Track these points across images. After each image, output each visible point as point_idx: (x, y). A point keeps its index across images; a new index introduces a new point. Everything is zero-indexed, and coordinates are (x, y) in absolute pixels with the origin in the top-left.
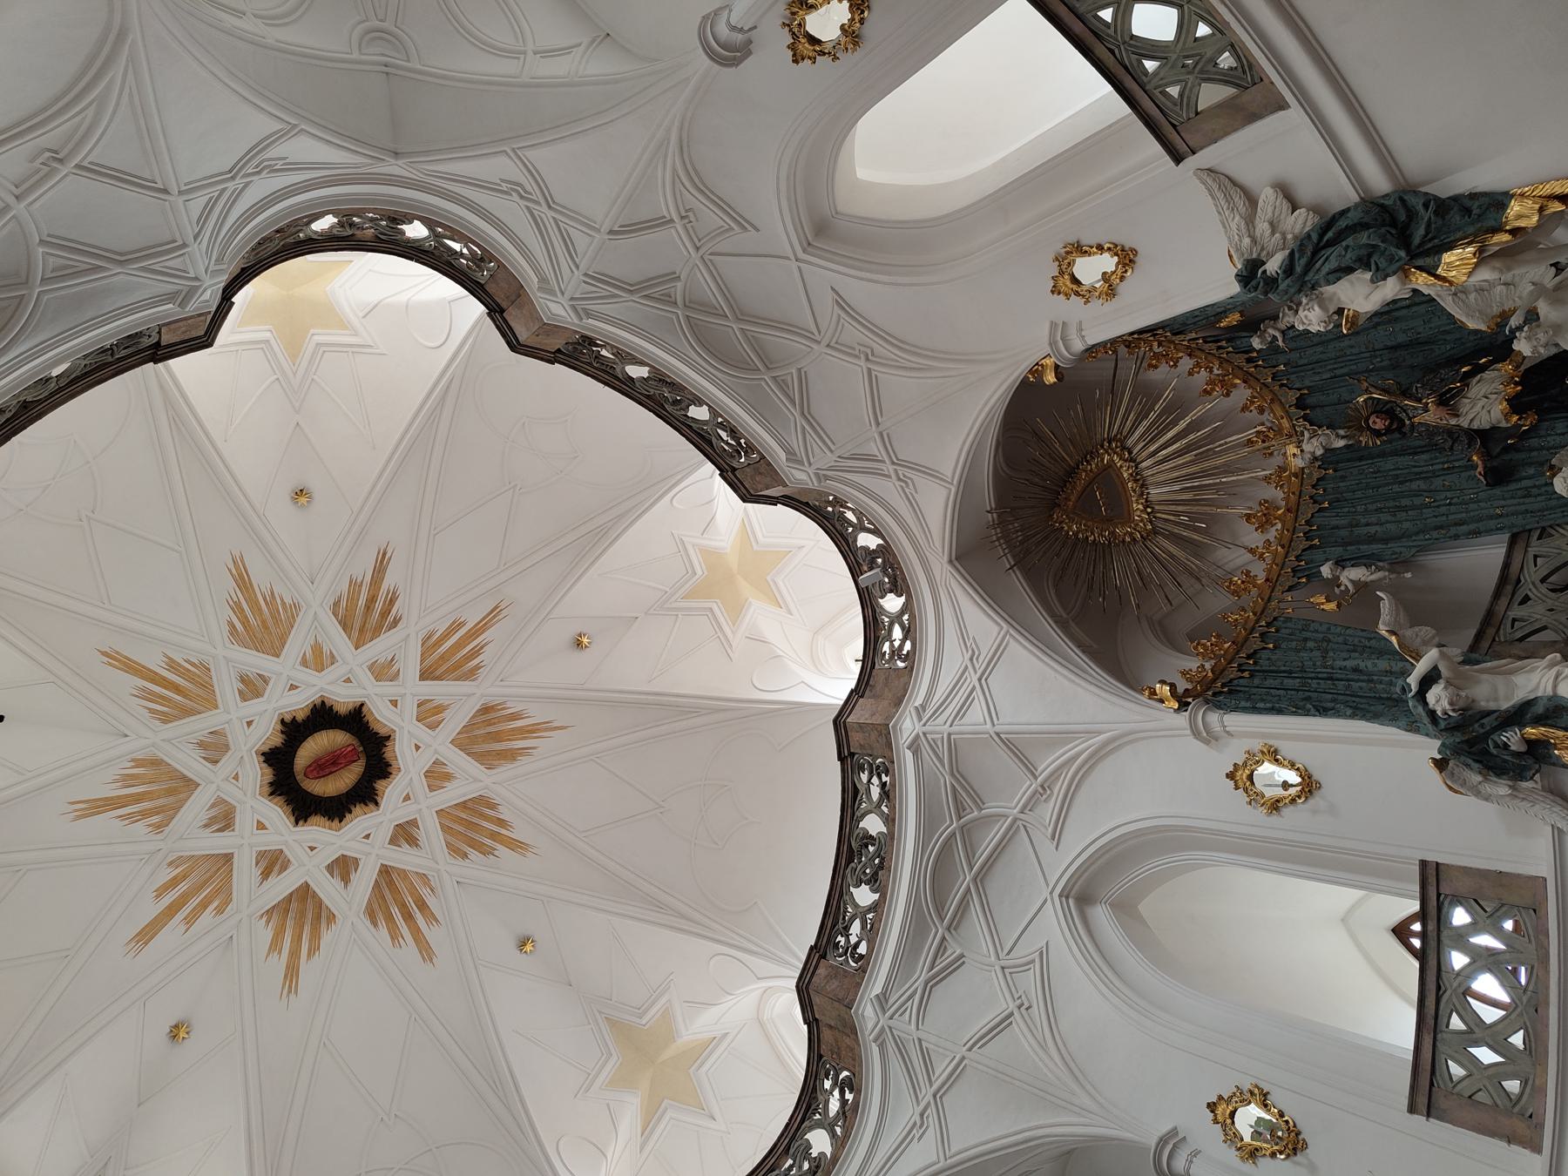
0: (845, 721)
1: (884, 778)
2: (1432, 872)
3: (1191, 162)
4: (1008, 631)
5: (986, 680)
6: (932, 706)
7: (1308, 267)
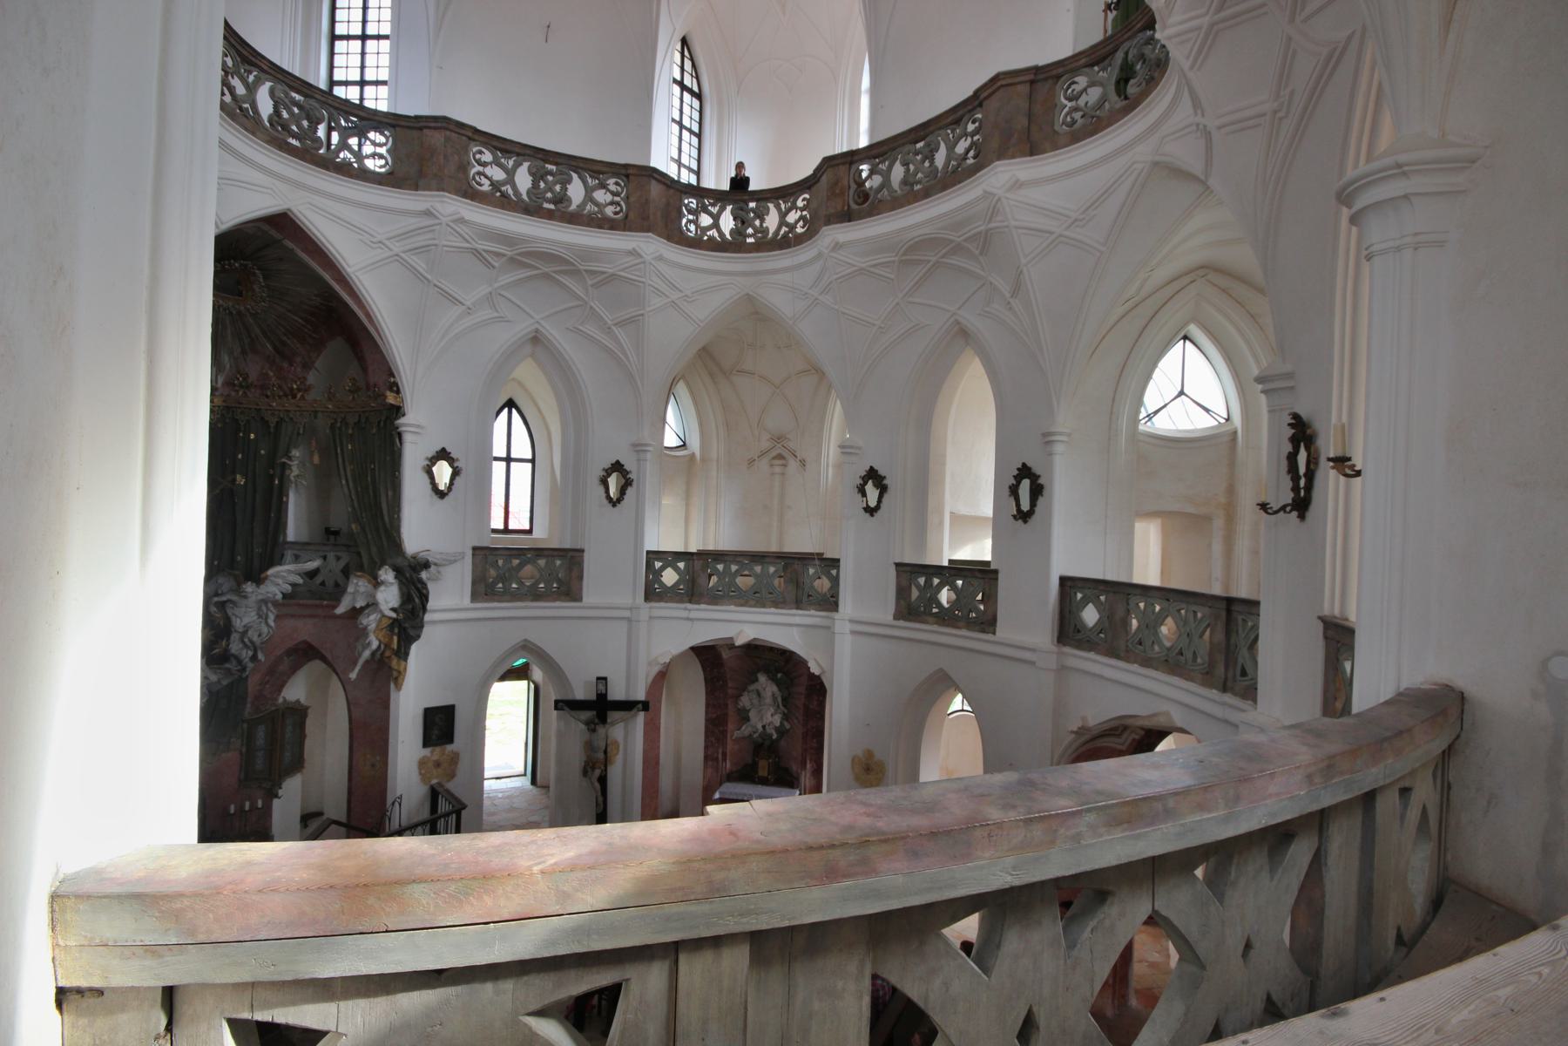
3: (470, 552)
7: (418, 589)
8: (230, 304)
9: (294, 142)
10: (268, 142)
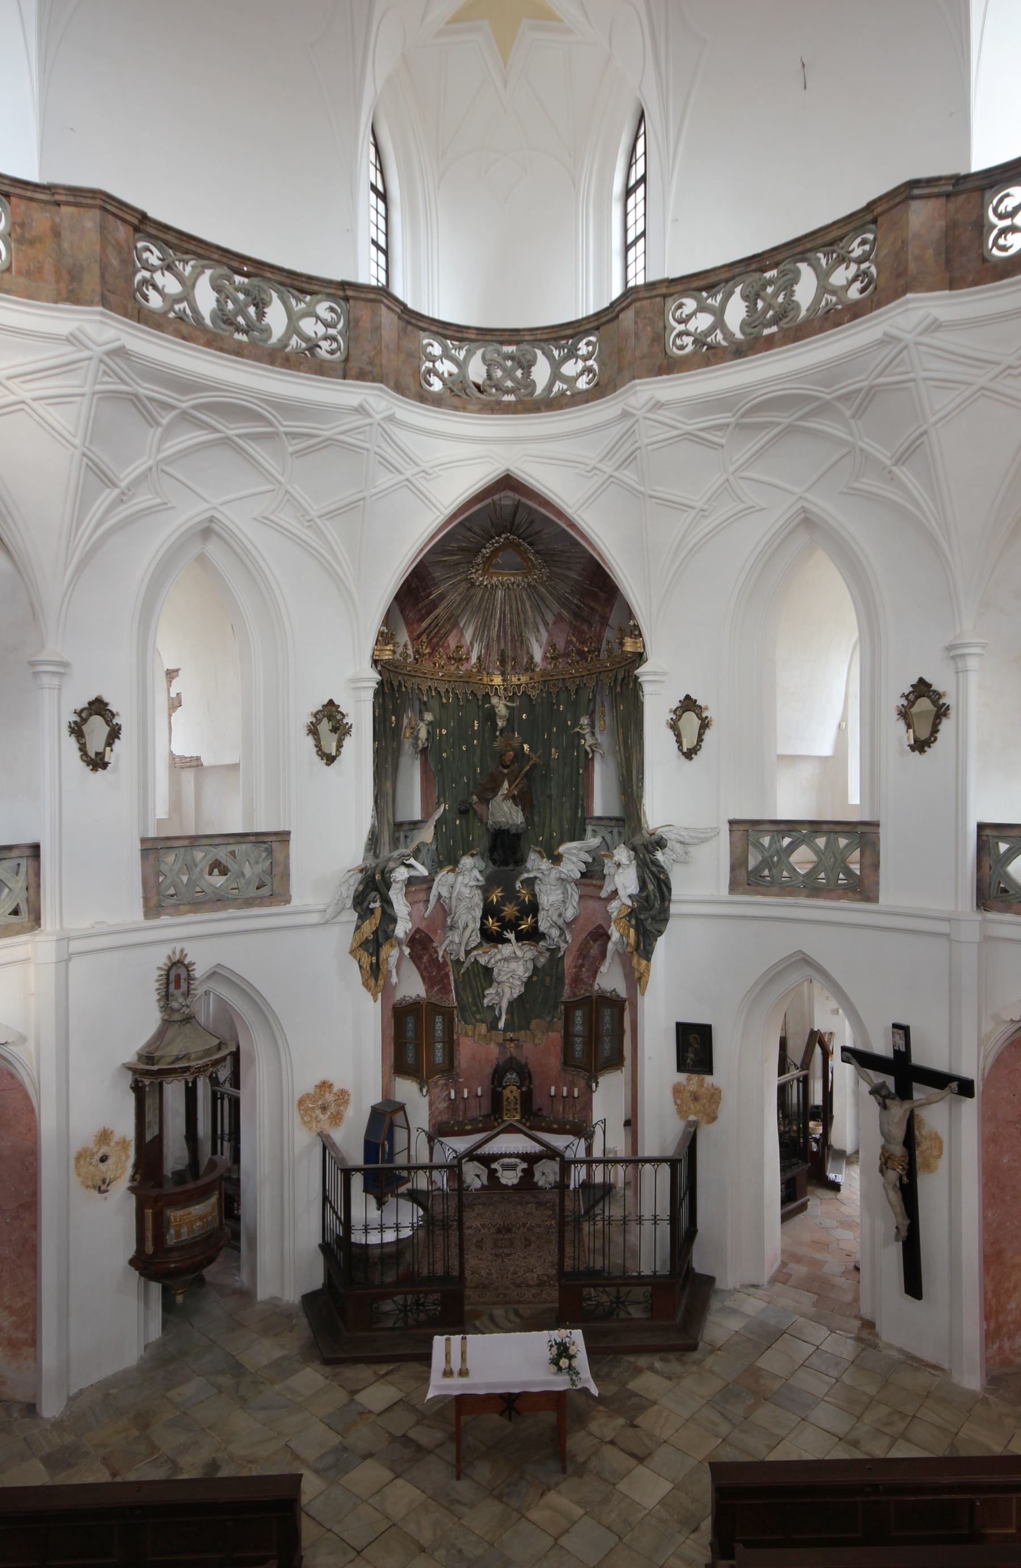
0: (382, 302)
1: (325, 345)
2: (285, 838)
4: (441, 513)
5: (406, 485)
6: (390, 426)
8: (520, 578)
9: (511, 398)
10: (480, 411)
